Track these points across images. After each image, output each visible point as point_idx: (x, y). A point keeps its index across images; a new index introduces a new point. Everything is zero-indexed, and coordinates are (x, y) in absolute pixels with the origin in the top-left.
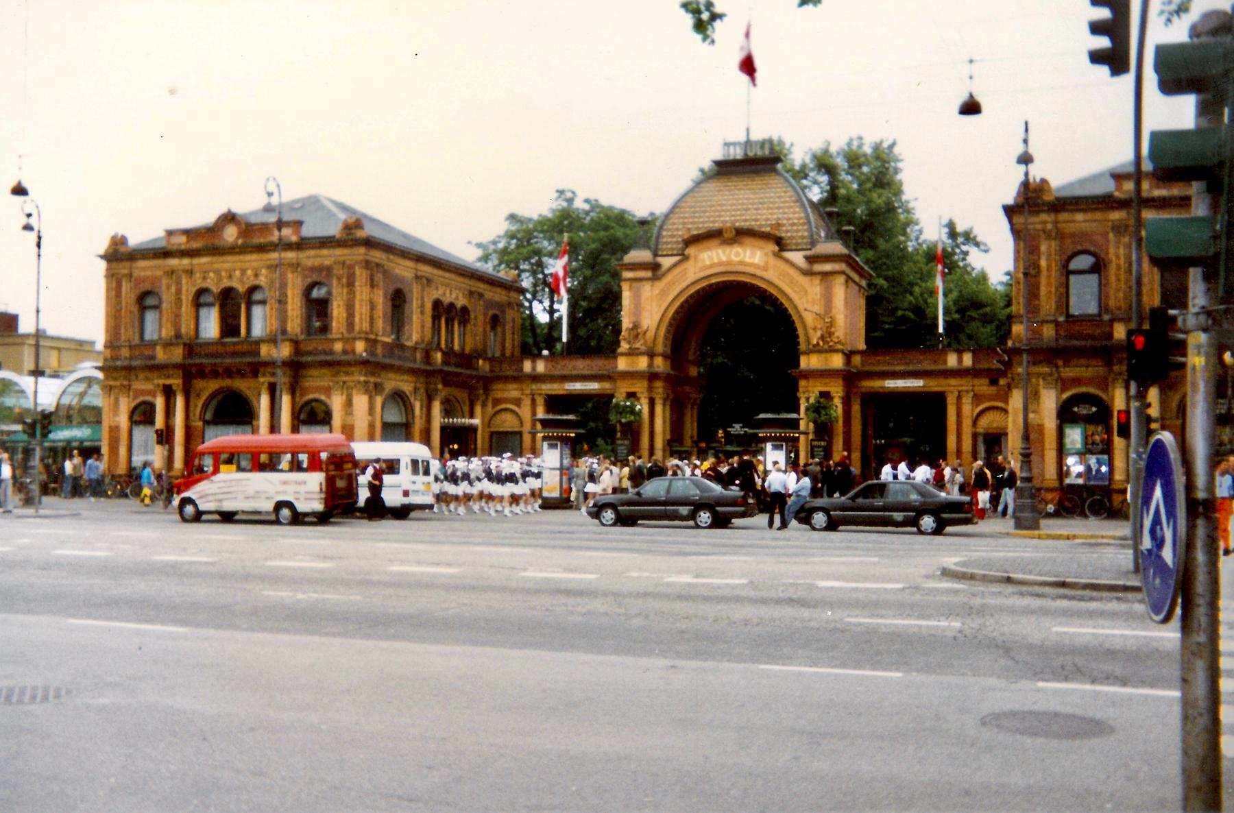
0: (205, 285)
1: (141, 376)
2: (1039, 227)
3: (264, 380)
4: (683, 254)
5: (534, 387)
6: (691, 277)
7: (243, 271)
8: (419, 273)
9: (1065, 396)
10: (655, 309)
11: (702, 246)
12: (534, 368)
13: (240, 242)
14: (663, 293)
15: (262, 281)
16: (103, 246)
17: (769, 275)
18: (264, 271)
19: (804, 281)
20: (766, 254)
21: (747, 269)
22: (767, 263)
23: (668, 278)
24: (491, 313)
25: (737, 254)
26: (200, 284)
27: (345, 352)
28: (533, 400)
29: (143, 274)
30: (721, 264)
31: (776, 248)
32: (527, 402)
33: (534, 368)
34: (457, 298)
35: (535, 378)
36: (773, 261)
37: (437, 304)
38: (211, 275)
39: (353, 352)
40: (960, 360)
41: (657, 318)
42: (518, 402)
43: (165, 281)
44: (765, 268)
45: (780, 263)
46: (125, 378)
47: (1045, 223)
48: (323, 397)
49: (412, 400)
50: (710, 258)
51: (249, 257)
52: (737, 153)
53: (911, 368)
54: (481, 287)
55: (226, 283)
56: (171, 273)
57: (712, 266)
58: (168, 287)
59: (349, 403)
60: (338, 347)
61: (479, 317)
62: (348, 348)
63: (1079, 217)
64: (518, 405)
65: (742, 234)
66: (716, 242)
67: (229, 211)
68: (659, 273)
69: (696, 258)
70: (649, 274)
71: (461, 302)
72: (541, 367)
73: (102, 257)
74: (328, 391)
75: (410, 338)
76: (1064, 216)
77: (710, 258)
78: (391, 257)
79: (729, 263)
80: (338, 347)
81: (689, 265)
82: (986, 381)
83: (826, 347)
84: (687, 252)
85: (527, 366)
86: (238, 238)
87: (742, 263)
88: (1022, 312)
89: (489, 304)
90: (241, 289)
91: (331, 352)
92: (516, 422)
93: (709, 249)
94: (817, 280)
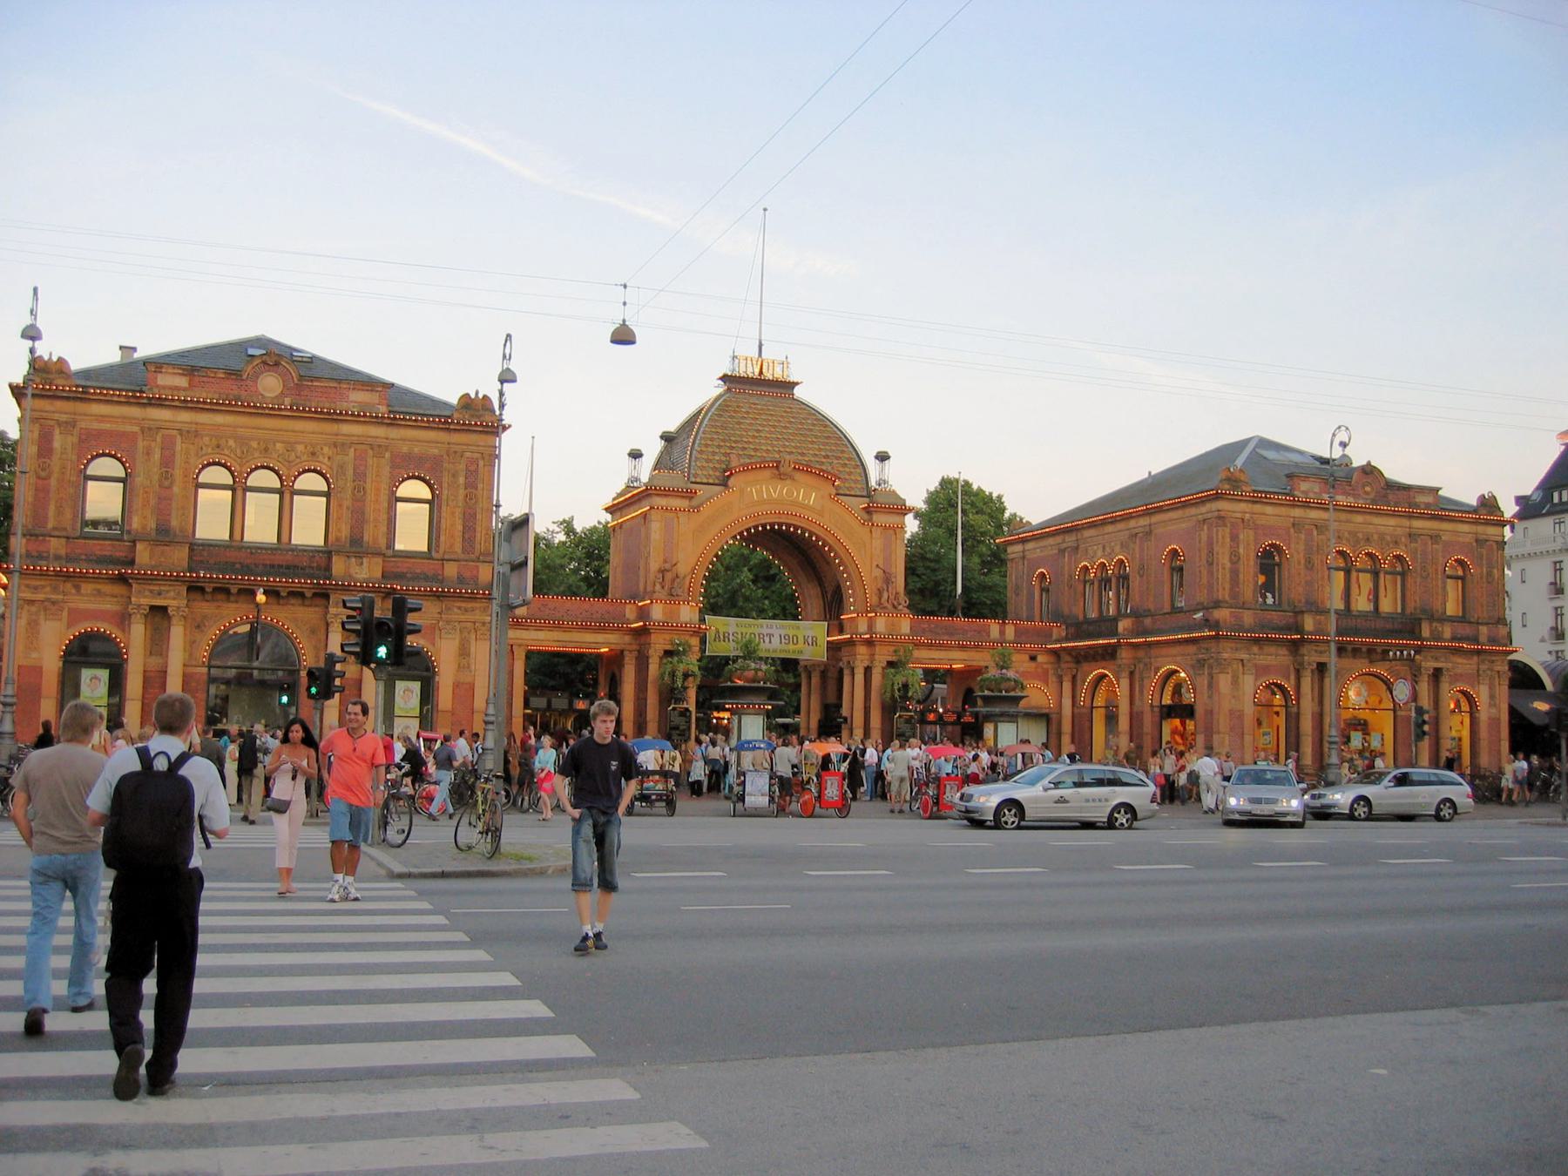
1: (87, 588)
4: (725, 485)
7: (290, 447)
11: (751, 476)
13: (287, 401)
17: (825, 521)
18: (326, 450)
19: (863, 532)
21: (798, 511)
23: (706, 510)
27: (461, 579)
29: (96, 426)
38: (231, 443)
40: (1002, 632)
43: (141, 444)
46: (55, 590)
50: (759, 492)
52: (752, 371)
56: (149, 430)
58: (148, 453)
59: (464, 652)
60: (451, 570)
62: (467, 574)
63: (1269, 510)
65: (807, 469)
66: (767, 473)
69: (742, 491)
76: (1258, 508)
77: (759, 492)
80: (451, 570)
82: (1027, 657)
84: (731, 482)
91: (442, 581)
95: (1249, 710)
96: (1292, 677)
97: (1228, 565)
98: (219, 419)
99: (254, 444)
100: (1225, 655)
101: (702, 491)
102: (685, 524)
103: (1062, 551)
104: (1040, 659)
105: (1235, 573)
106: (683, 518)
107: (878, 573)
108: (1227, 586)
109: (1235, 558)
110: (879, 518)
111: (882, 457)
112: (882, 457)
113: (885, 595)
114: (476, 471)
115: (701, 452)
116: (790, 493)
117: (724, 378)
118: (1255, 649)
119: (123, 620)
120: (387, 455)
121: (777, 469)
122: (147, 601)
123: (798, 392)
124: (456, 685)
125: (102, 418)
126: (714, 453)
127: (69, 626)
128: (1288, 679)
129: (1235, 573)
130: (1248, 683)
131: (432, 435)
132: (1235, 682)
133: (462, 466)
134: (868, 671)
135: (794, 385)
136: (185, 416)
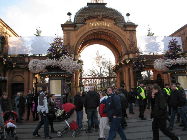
10: (75, 40)
14: (78, 35)
17: (113, 30)
19: (124, 33)
20: (112, 24)
22: (112, 27)
23: (79, 30)
30: (97, 26)
31: (115, 23)
36: (114, 26)
41: (76, 43)
45: (116, 27)
57: (95, 27)
66: (96, 20)
68: (76, 28)
70: (73, 28)
77: (94, 24)
79: (99, 26)
81: (86, 26)
83: (135, 52)
84: (86, 22)
87: (104, 26)
92: (22, 80)
93: (92, 22)
94: (128, 32)
102: (72, 34)
106: (72, 32)
107: (129, 43)
111: (128, 15)
112: (128, 15)
113: (132, 48)
116: (102, 24)
117: (88, 4)
123: (107, 6)
134: (129, 69)
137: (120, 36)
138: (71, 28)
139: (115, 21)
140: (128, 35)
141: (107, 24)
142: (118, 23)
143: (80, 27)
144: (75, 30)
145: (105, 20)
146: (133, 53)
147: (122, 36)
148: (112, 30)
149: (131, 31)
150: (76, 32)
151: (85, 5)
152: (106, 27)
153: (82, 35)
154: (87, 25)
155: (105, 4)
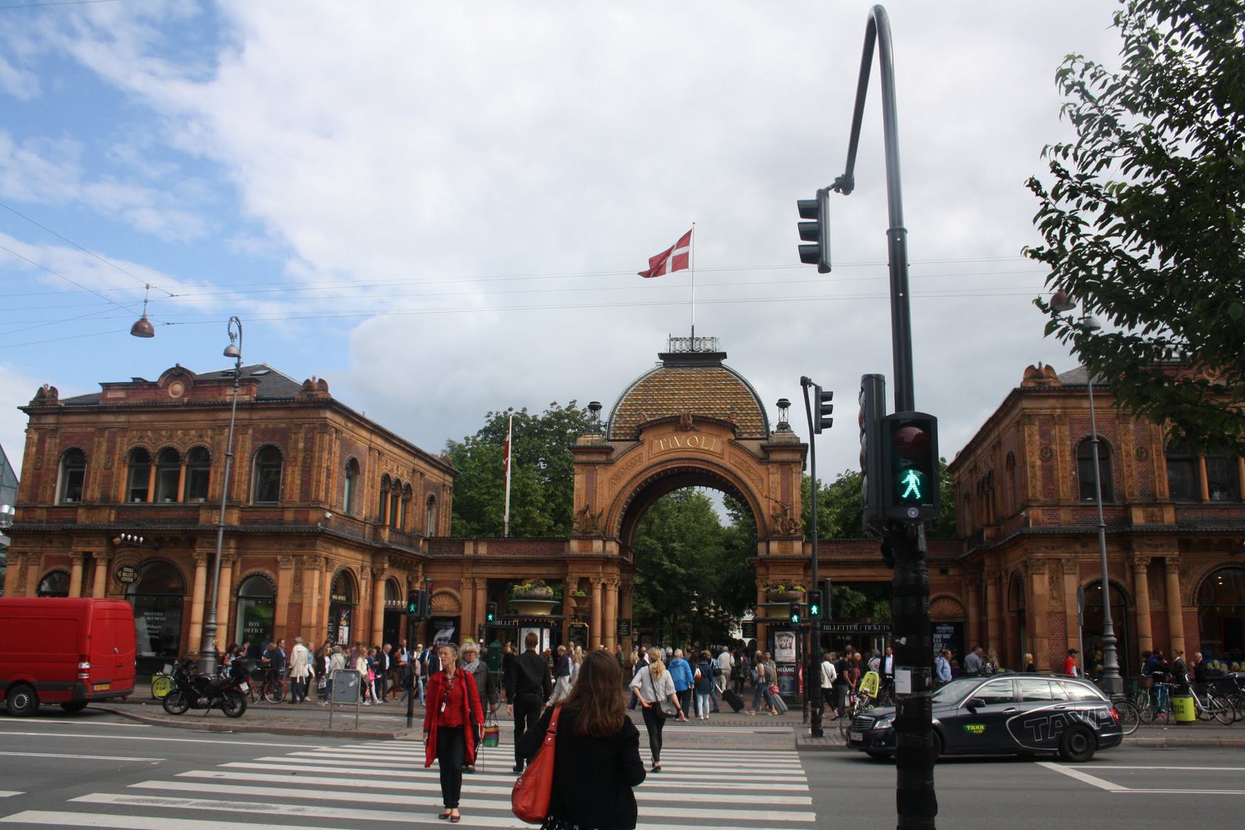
0: (142, 445)
2: (1048, 412)
3: (200, 551)
4: (637, 439)
5: (475, 570)
6: (646, 463)
8: (373, 445)
9: (1084, 583)
12: (475, 551)
13: (186, 400)
14: (616, 478)
15: (207, 442)
16: (28, 396)
17: (726, 462)
18: (209, 432)
19: (760, 469)
23: (621, 463)
24: (430, 493)
25: (693, 441)
26: (136, 443)
27: (295, 522)
28: (474, 584)
30: (676, 450)
31: (733, 437)
32: (467, 585)
33: (475, 551)
34: (402, 475)
35: (477, 561)
36: (728, 449)
37: (386, 478)
39: (306, 521)
42: (458, 585)
44: (721, 456)
45: (736, 452)
47: (1055, 408)
48: (267, 572)
49: (359, 578)
51: (193, 417)
52: (684, 347)
53: (861, 557)
54: (422, 465)
55: (165, 443)
60: (289, 516)
61: (419, 497)
64: (458, 590)
67: (177, 366)
68: (614, 456)
69: (651, 443)
70: (603, 458)
71: (405, 480)
72: (483, 550)
73: (25, 410)
74: (275, 566)
75: (360, 512)
76: (1071, 402)
78: (350, 425)
79: (685, 450)
81: (643, 450)
84: (641, 438)
85: (469, 549)
86: (184, 396)
88: (1039, 496)
89: (428, 485)
90: (183, 450)
91: (281, 522)
92: (455, 608)
95: (1074, 609)
96: (1128, 575)
97: (1038, 463)
98: (144, 417)
99: (164, 433)
100: (1040, 555)
101: (619, 447)
102: (603, 476)
103: (971, 471)
104: (951, 572)
105: (1049, 472)
108: (1039, 485)
109: (1047, 455)
110: (775, 456)
114: (313, 437)
115: (620, 416)
117: (662, 356)
118: (1078, 548)
119: (70, 563)
120: (250, 432)
121: (677, 424)
122: (80, 549)
124: (291, 605)
125: (73, 424)
126: (631, 416)
127: (45, 568)
128: (1123, 577)
129: (1049, 472)
130: (1071, 584)
131: (281, 414)
132: (1055, 583)
133: (302, 435)
135: (724, 355)
136: (122, 418)
137: (745, 479)
138: (595, 458)
139: (734, 432)
140: (775, 477)
141: (708, 445)
142: (745, 436)
143: (624, 453)
144: (610, 463)
145: (704, 429)
146: (780, 540)
147: (753, 480)
148: (721, 462)
149: (783, 463)
150: (613, 470)
151: (652, 363)
152: (704, 451)
153: (628, 477)
154: (646, 447)
155: (724, 355)
